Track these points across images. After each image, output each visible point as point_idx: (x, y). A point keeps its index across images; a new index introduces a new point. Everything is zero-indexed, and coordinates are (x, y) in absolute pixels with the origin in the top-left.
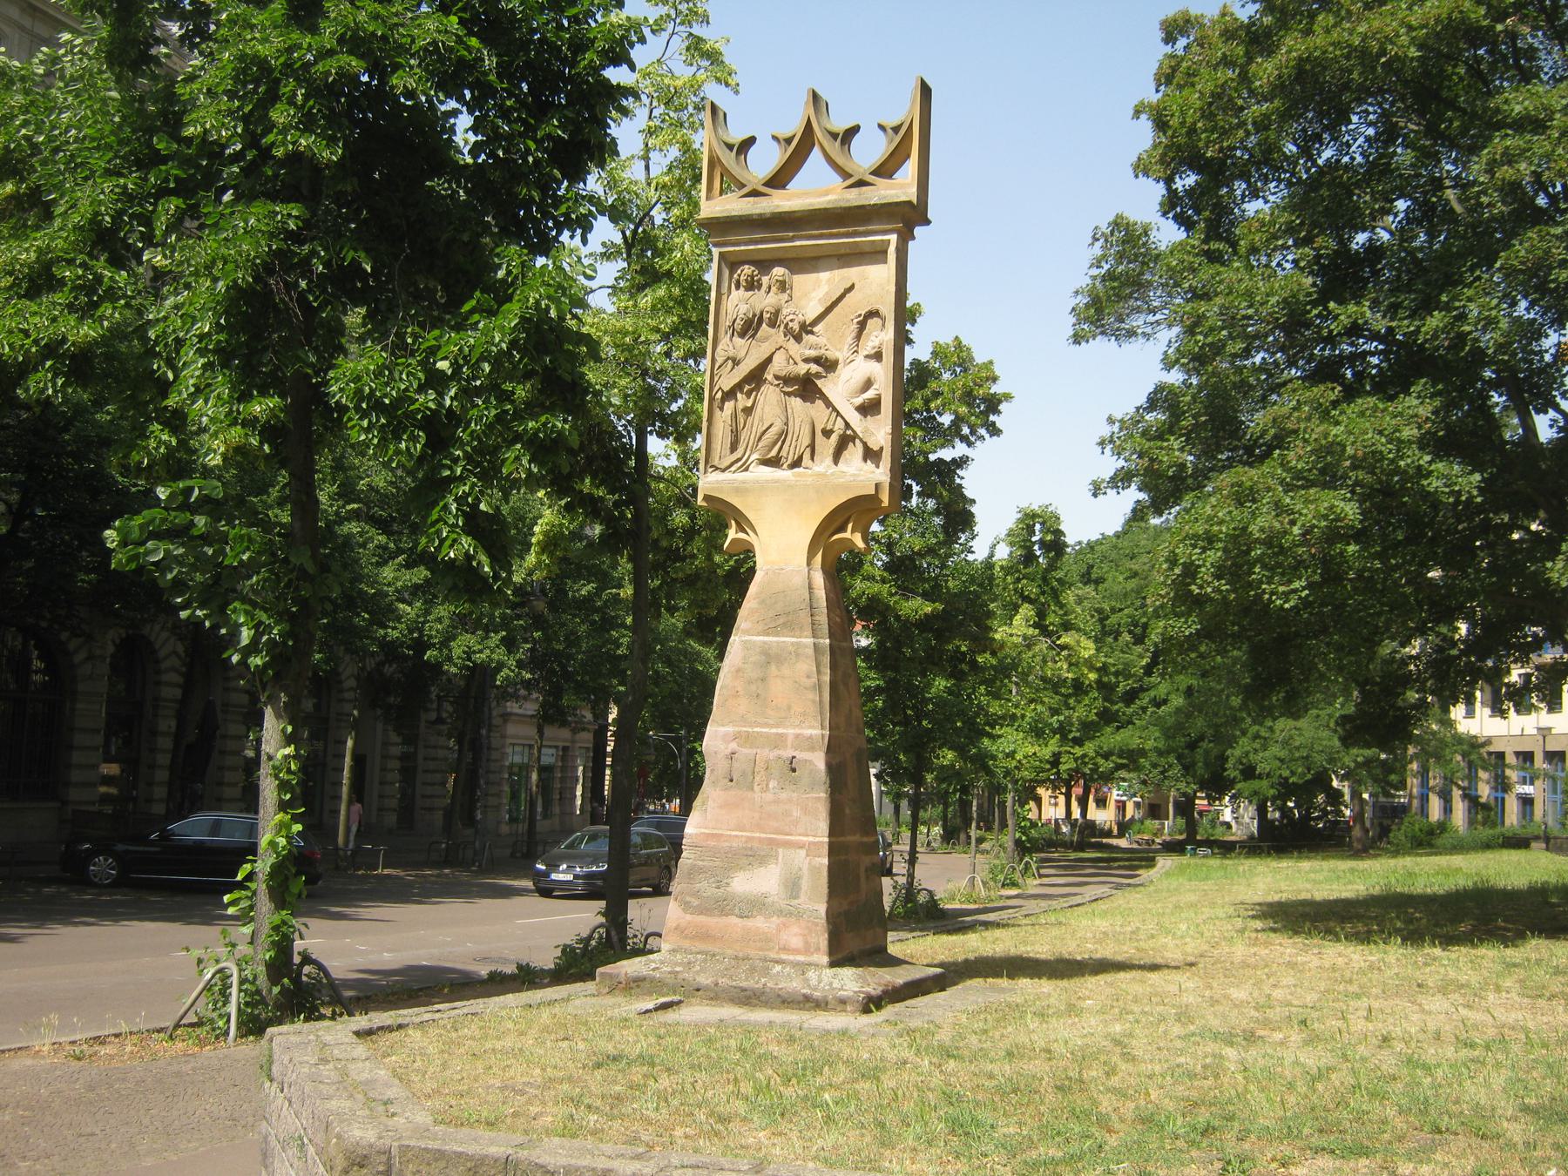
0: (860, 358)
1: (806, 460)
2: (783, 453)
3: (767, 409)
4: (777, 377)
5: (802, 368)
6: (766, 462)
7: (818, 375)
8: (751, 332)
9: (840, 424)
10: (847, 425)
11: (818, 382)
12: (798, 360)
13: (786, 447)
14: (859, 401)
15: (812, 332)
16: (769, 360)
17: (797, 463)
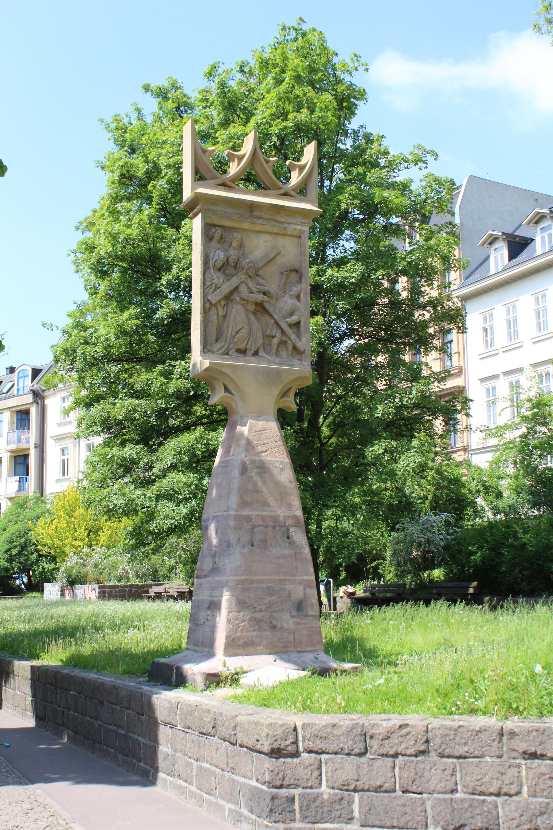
0: (287, 295)
1: (262, 353)
2: (249, 346)
3: (238, 318)
4: (243, 300)
5: (260, 297)
6: (239, 351)
7: (266, 302)
8: (223, 269)
9: (279, 334)
10: (283, 332)
11: (266, 305)
12: (253, 289)
13: (250, 343)
14: (289, 320)
15: (258, 275)
16: (236, 288)
17: (256, 353)
